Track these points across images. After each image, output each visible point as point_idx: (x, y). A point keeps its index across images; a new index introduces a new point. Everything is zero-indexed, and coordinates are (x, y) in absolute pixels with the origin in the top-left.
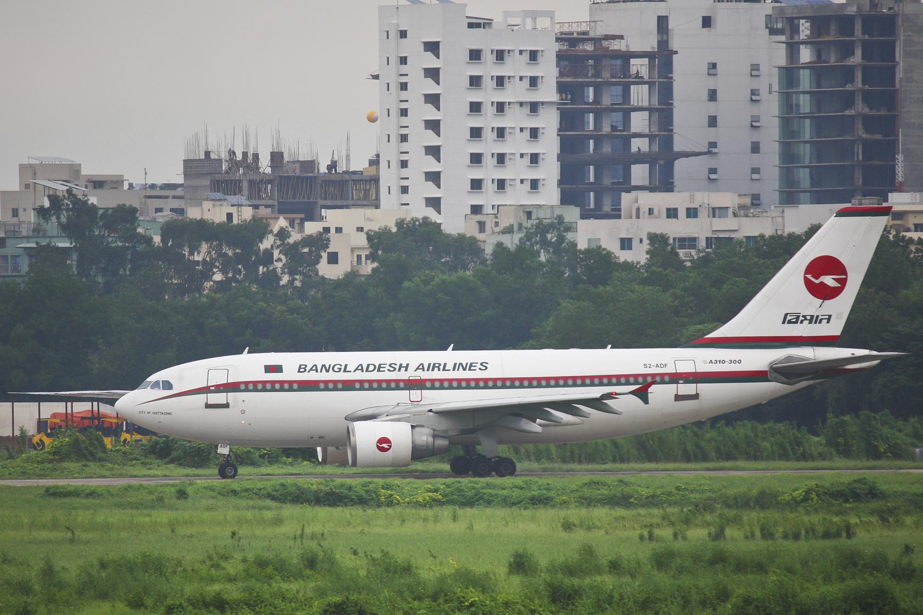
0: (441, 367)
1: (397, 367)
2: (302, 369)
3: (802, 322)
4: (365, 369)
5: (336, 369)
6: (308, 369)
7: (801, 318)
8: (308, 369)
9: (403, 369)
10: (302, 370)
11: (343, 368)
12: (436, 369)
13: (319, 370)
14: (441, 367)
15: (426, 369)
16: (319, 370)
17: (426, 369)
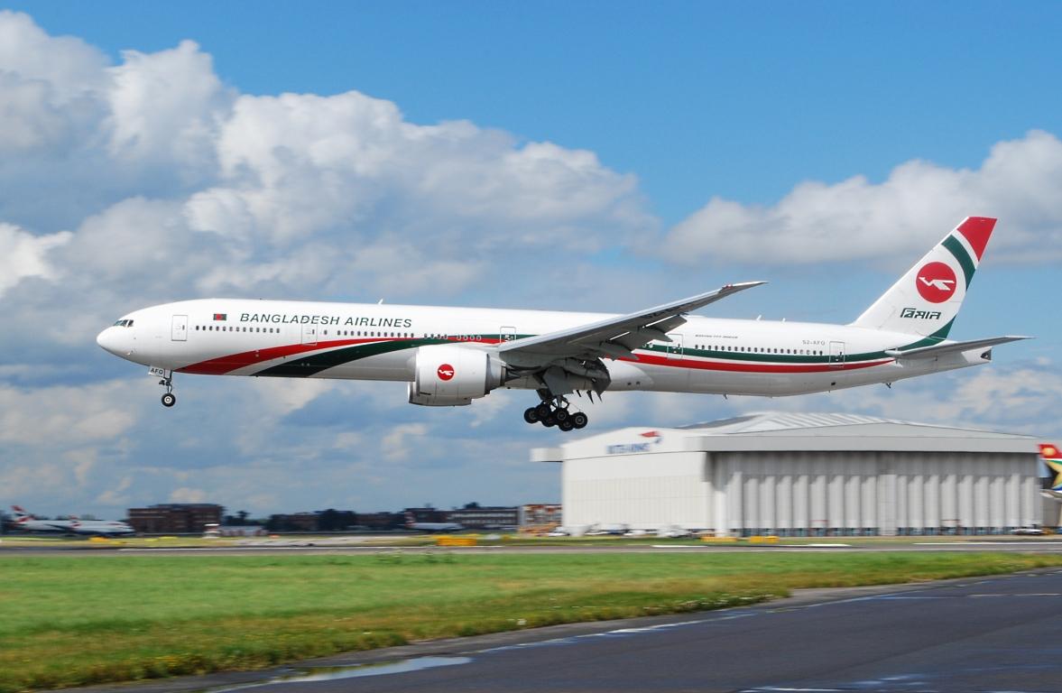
0: (369, 323)
1: (329, 320)
2: (244, 317)
3: (916, 317)
4: (299, 321)
5: (275, 320)
6: (250, 318)
7: (916, 313)
8: (250, 318)
9: (334, 322)
10: (244, 319)
11: (282, 319)
12: (364, 324)
13: (260, 319)
14: (369, 323)
15: (354, 323)
16: (260, 319)
17: (354, 323)
